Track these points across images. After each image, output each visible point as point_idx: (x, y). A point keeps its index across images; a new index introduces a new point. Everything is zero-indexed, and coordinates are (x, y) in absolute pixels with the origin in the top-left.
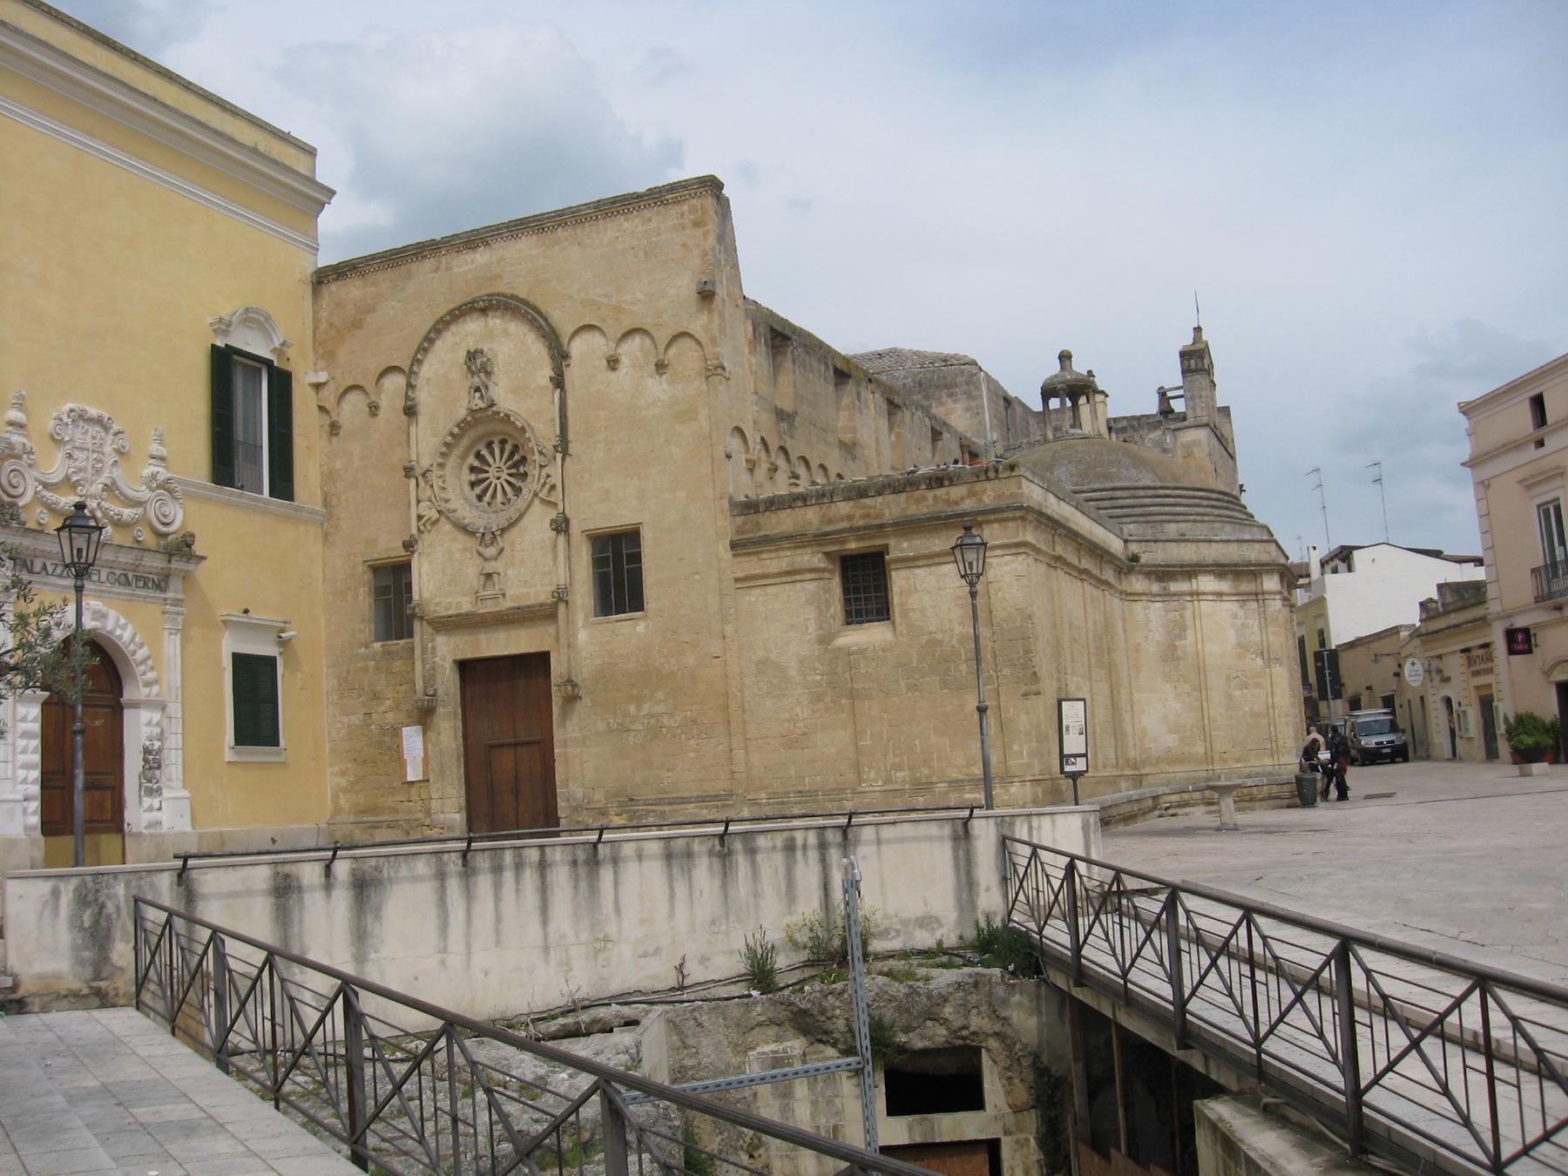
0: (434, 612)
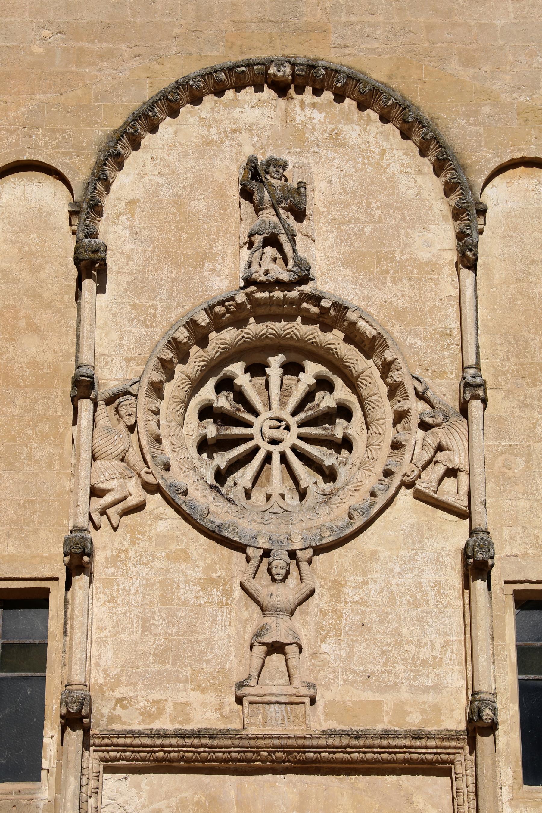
0: (112, 719)
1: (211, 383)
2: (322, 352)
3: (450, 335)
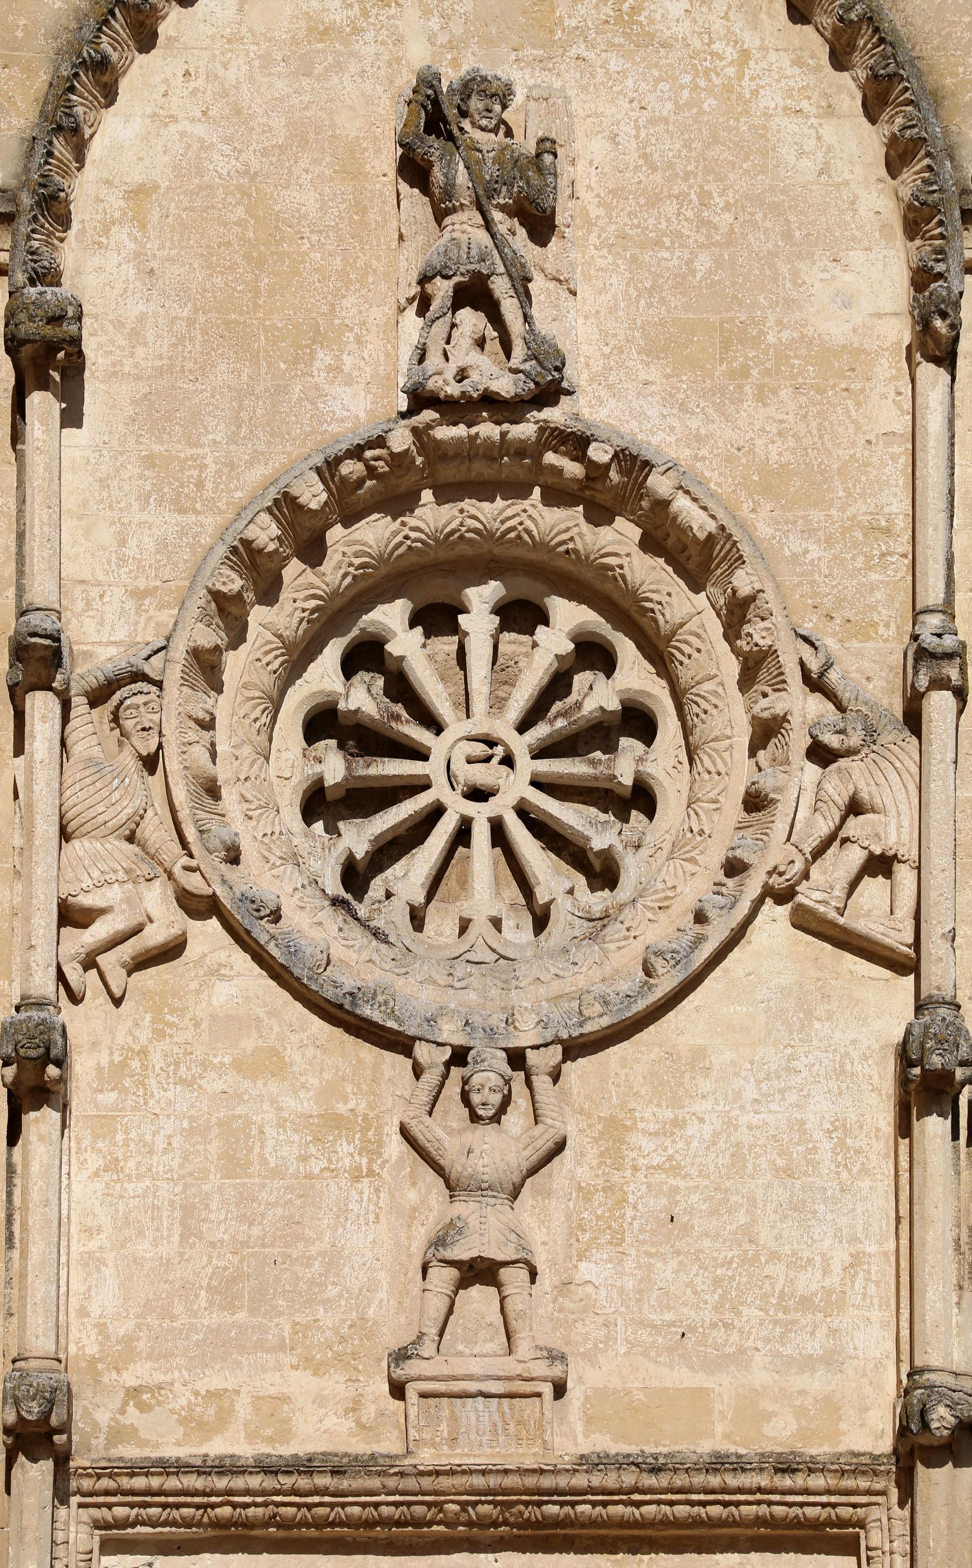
0: (117, 1434)
1: (333, 652)
2: (589, 575)
3: (888, 531)
